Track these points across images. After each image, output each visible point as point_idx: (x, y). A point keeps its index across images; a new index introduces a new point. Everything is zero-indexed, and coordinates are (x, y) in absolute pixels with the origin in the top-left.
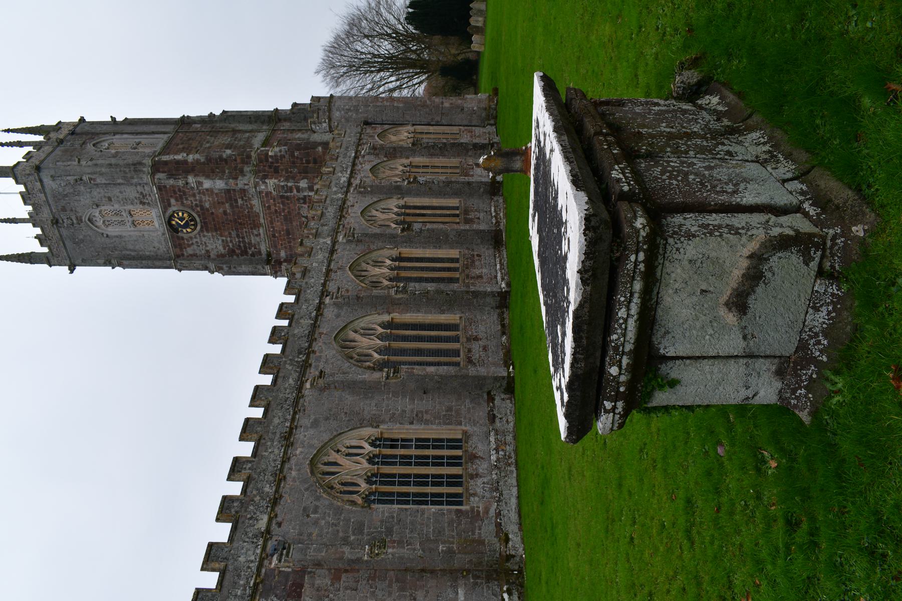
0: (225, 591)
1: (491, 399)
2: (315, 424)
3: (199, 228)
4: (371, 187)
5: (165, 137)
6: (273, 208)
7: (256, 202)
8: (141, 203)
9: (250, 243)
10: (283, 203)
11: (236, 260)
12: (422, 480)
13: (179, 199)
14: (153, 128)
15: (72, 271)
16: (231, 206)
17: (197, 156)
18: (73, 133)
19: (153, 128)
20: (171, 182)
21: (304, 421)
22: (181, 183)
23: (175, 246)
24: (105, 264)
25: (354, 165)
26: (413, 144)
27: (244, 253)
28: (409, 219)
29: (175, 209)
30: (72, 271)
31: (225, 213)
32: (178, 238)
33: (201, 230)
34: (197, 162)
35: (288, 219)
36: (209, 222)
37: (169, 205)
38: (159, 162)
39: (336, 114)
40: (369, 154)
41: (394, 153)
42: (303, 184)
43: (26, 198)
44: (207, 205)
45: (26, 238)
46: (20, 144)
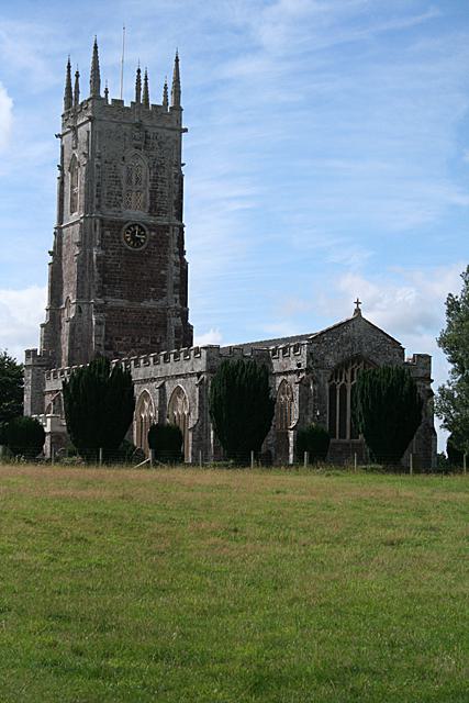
3: (129, 248)
6: (148, 316)
7: (149, 304)
8: (151, 209)
29: (147, 233)
31: (142, 274)
33: (126, 249)
37: (151, 230)
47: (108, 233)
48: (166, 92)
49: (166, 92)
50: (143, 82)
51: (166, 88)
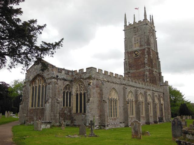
0: (97, 73)
1: (123, 123)
2: (118, 88)
4: (154, 96)
5: (154, 50)
8: (140, 46)
9: (132, 68)
10: (142, 75)
11: (128, 65)
12: (111, 108)
13: (141, 53)
14: (155, 46)
15: (123, 30)
16: (141, 64)
17: (152, 57)
18: (153, 30)
19: (155, 46)
20: (146, 52)
21: (119, 85)
22: (146, 54)
23: (130, 52)
24: (125, 37)
25: (156, 91)
26: (161, 104)
27: (130, 67)
28: (129, 102)
29: (139, 52)
30: (123, 30)
32: (132, 53)
34: (151, 57)
35: (138, 76)
36: (136, 60)
37: (140, 51)
38: (150, 49)
39: (165, 87)
40: (159, 95)
41: (160, 100)
42: (148, 80)
43: (140, 21)
44: (141, 59)
45: (130, 21)
46: (150, 20)
47: (130, 55)
48: (150, 17)
49: (150, 17)
50: (151, 17)
51: (150, 16)
